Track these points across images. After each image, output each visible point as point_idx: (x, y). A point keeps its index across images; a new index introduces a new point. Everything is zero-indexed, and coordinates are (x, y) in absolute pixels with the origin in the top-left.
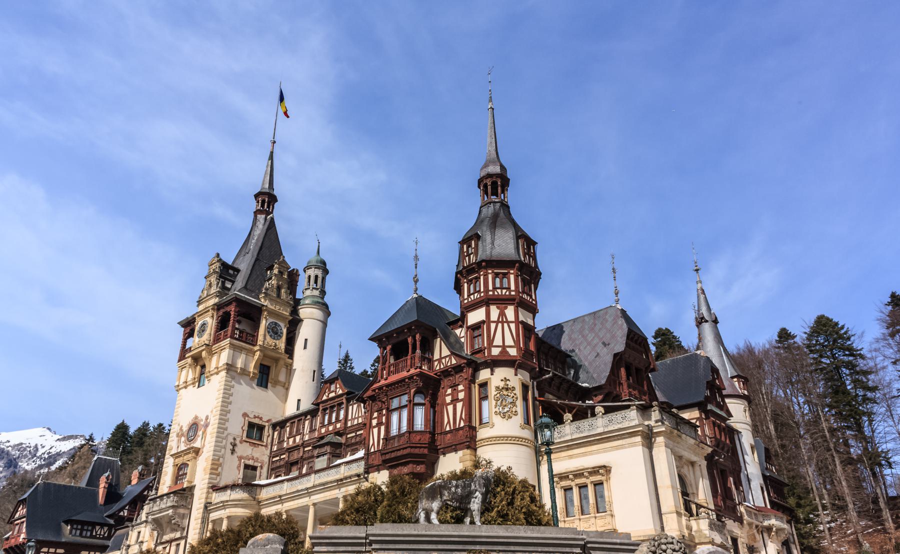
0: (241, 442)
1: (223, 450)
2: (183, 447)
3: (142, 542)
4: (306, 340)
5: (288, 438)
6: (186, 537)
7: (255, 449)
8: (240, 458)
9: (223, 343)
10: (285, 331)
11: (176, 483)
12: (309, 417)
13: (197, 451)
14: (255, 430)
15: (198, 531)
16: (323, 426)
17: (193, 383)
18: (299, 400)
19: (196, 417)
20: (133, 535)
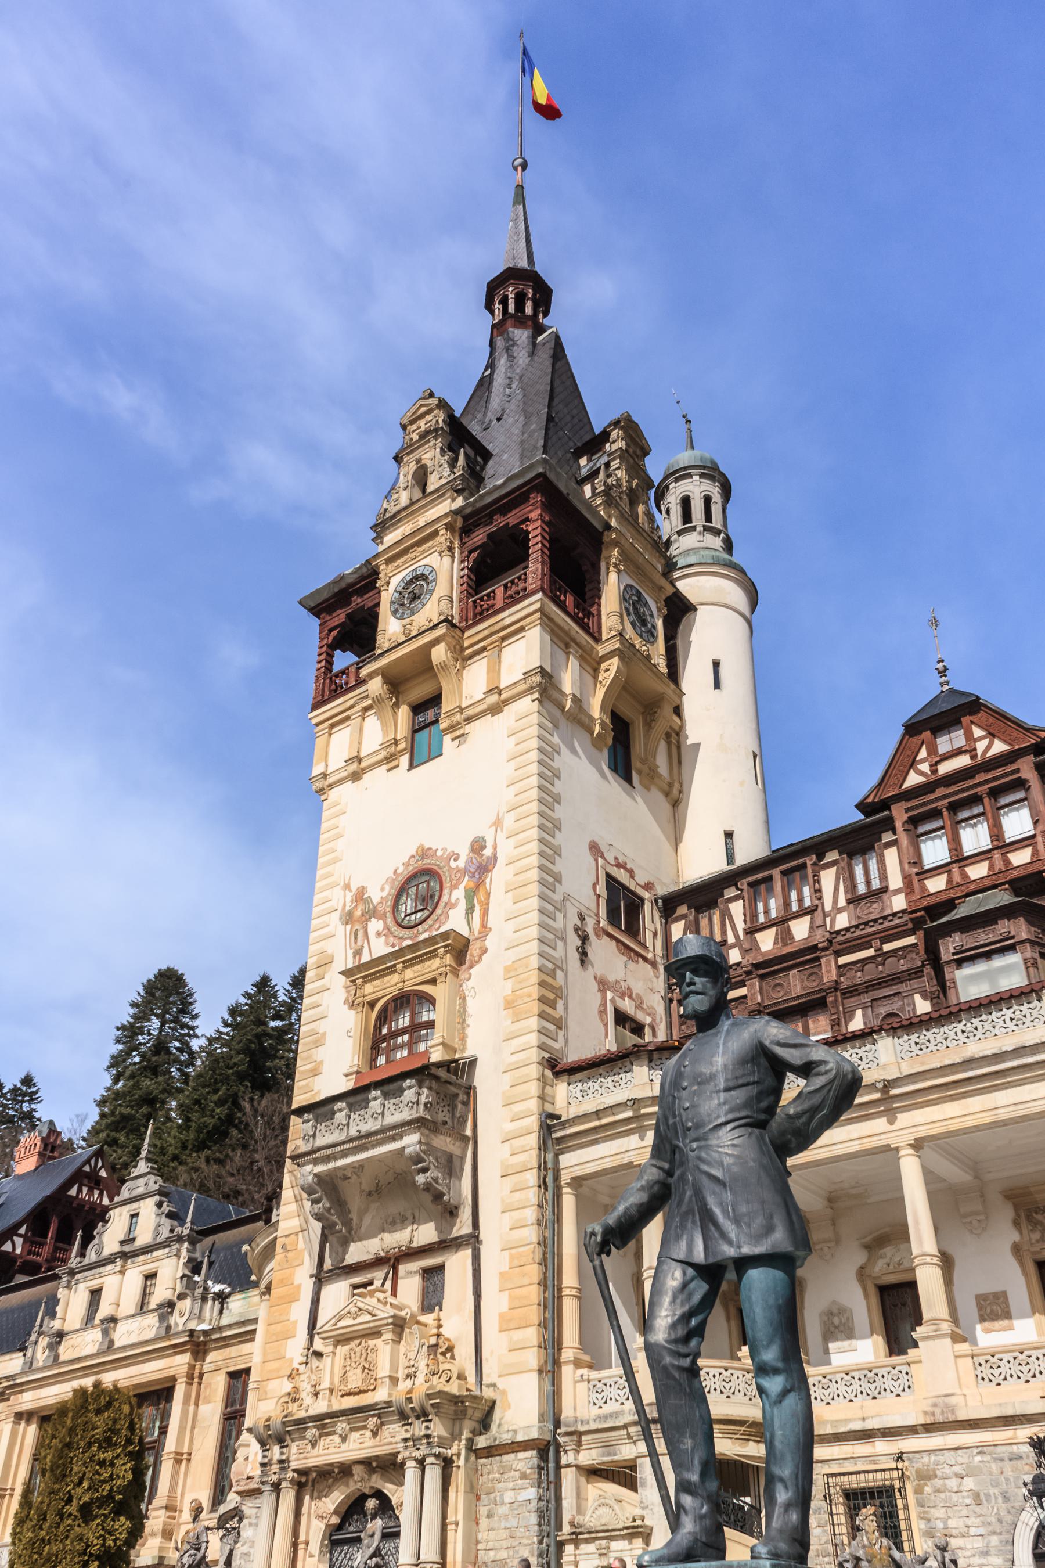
0: (597, 935)
1: (560, 944)
2: (379, 947)
3: (113, 1320)
4: (716, 664)
5: (751, 932)
6: (473, 1240)
7: (631, 965)
8: (603, 985)
9: (508, 617)
10: (660, 624)
11: (373, 1061)
12: (832, 856)
13: (460, 951)
14: (623, 906)
15: (531, 1214)
16: (925, 873)
17: (390, 758)
18: (729, 835)
19: (424, 853)
20: (73, 1302)
